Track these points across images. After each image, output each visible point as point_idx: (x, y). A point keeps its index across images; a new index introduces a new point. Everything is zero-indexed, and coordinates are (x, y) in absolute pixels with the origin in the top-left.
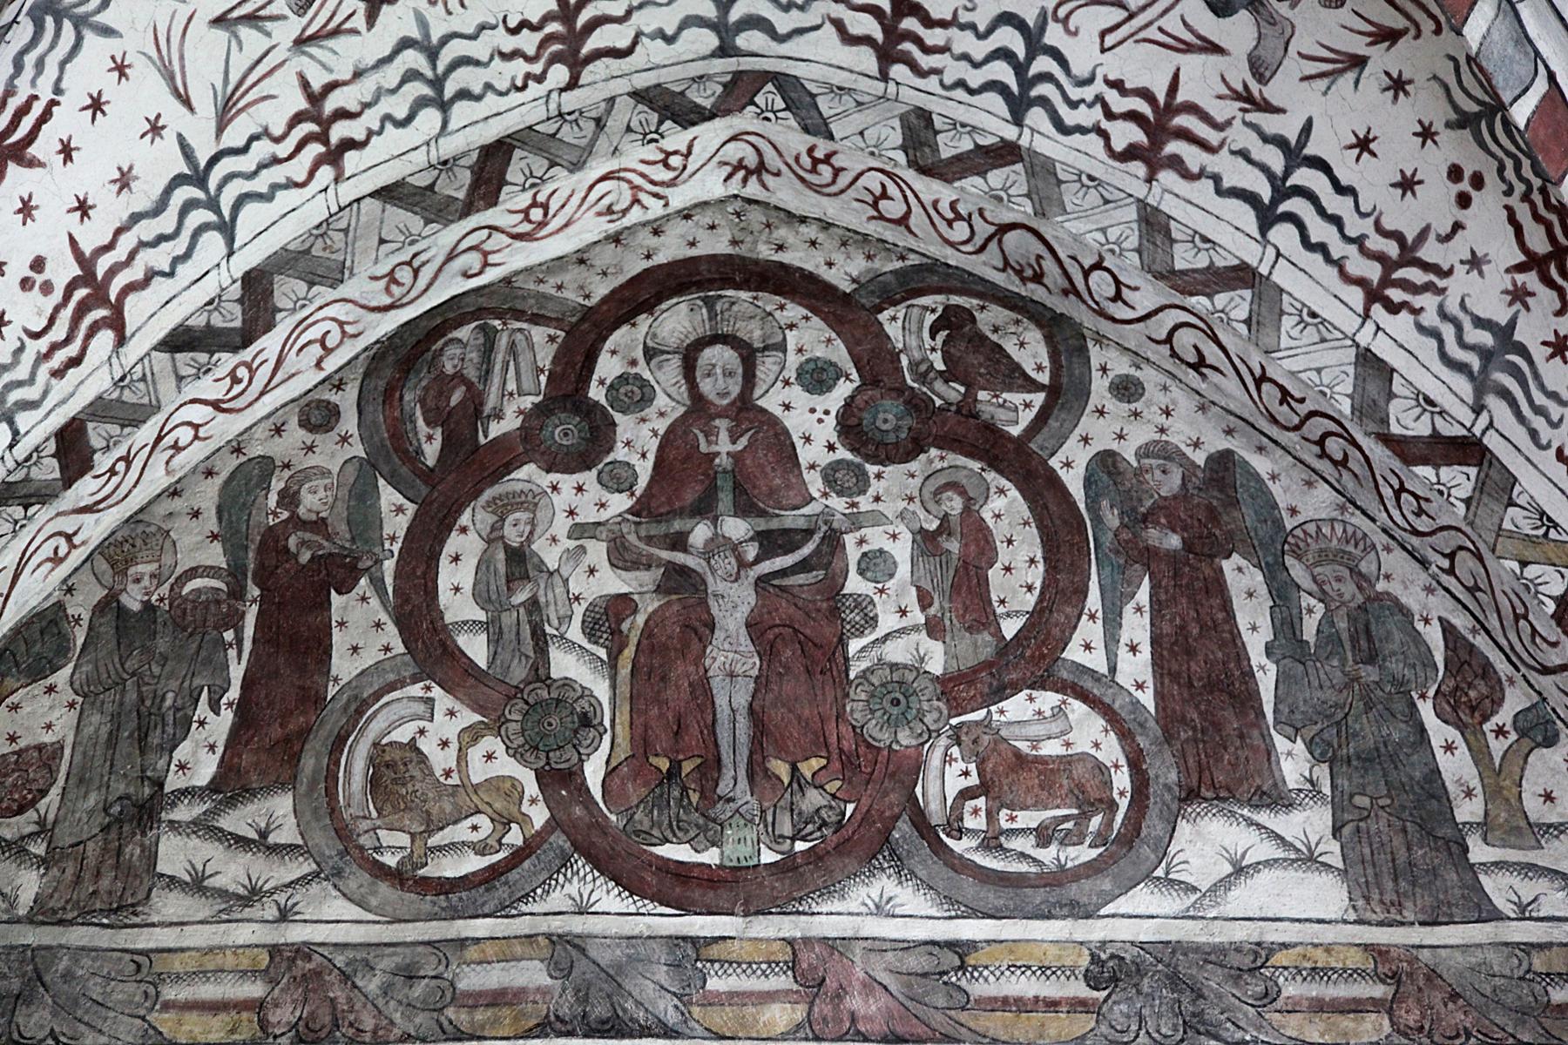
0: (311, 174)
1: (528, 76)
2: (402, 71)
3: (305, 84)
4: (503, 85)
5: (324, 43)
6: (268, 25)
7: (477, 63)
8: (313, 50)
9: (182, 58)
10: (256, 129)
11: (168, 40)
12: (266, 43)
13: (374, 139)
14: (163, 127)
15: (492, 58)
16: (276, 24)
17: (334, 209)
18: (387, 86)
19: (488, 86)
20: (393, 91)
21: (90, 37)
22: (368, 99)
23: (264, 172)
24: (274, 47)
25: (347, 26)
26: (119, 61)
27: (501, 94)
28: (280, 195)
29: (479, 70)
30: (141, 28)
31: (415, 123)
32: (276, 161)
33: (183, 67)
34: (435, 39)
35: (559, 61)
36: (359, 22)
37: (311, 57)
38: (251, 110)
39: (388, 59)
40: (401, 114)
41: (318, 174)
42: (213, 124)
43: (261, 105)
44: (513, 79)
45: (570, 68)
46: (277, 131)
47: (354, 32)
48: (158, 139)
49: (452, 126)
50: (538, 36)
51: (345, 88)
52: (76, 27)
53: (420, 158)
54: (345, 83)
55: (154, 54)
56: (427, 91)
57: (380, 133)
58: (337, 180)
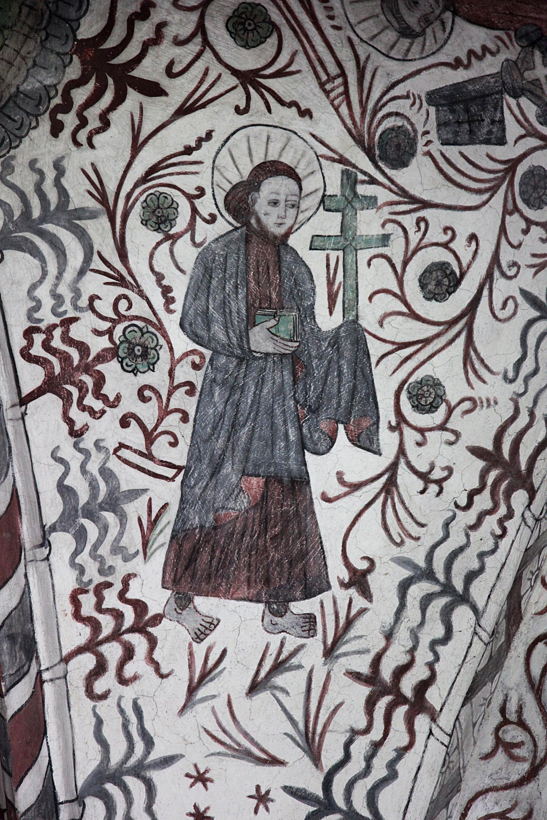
0: (411, 732)
1: (501, 522)
2: (417, 604)
3: (356, 676)
4: (489, 545)
5: (347, 637)
6: (294, 661)
7: (461, 549)
8: (343, 649)
9: (246, 735)
10: (344, 738)
11: (224, 731)
12: (303, 675)
13: (437, 667)
14: (268, 792)
15: (468, 536)
16: (299, 656)
17: (446, 740)
18: (416, 624)
19: (481, 556)
20: (422, 623)
21: (156, 776)
22: (409, 644)
23: (375, 761)
24: (311, 671)
25: (353, 612)
26: (195, 774)
27: (493, 551)
28: (400, 767)
29: (467, 552)
30: (194, 739)
31: (455, 629)
32: (377, 746)
33: (252, 741)
34: (422, 564)
35: (513, 491)
36: (360, 602)
37: (345, 654)
38: (330, 728)
39: (402, 606)
40: (440, 632)
41: (417, 727)
42: (307, 760)
43: (336, 718)
44: (493, 534)
45: (523, 487)
46: (362, 724)
47: (362, 611)
48: (270, 805)
49: (480, 605)
50: (487, 492)
51: (388, 653)
52: (138, 776)
53: (478, 648)
54: (385, 650)
55: (221, 749)
56: (442, 602)
57: (437, 658)
58: (434, 719)
